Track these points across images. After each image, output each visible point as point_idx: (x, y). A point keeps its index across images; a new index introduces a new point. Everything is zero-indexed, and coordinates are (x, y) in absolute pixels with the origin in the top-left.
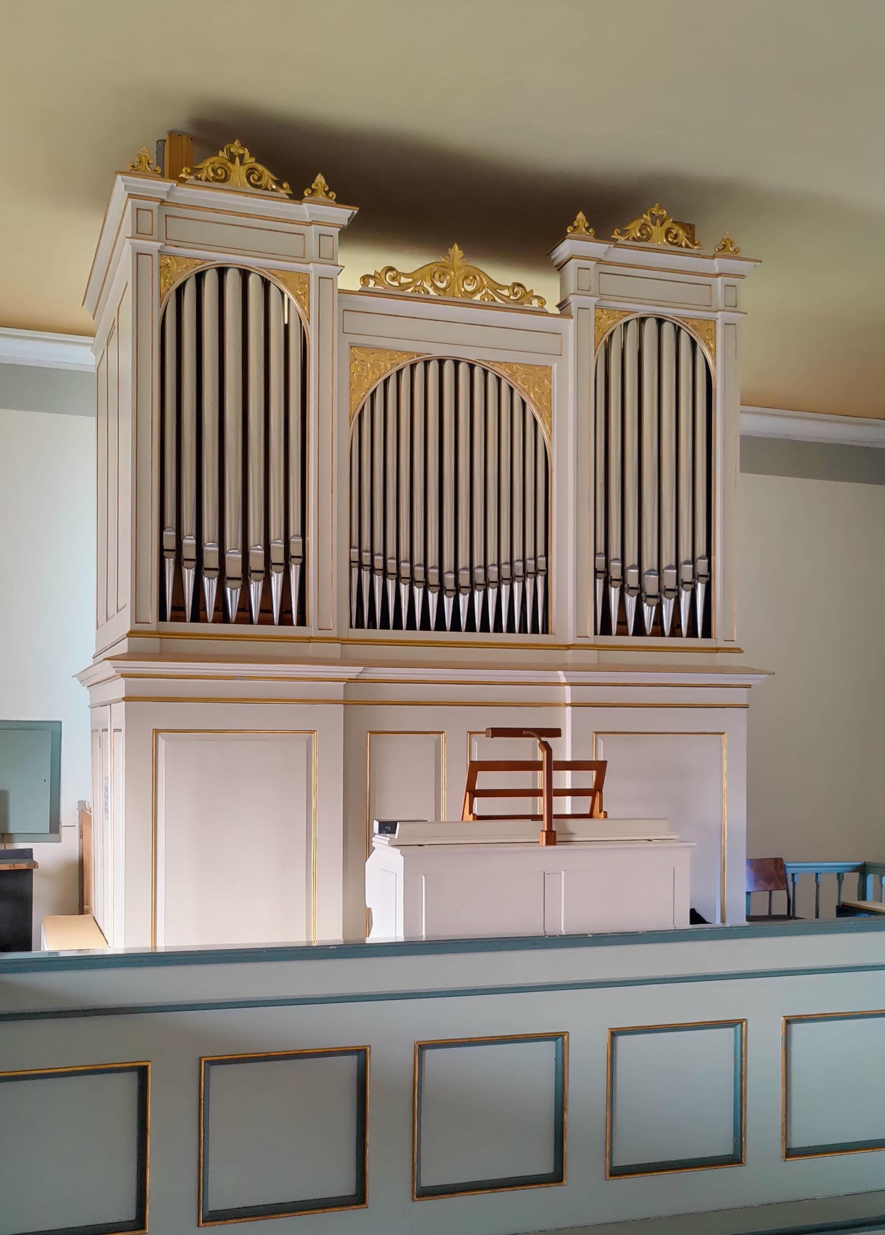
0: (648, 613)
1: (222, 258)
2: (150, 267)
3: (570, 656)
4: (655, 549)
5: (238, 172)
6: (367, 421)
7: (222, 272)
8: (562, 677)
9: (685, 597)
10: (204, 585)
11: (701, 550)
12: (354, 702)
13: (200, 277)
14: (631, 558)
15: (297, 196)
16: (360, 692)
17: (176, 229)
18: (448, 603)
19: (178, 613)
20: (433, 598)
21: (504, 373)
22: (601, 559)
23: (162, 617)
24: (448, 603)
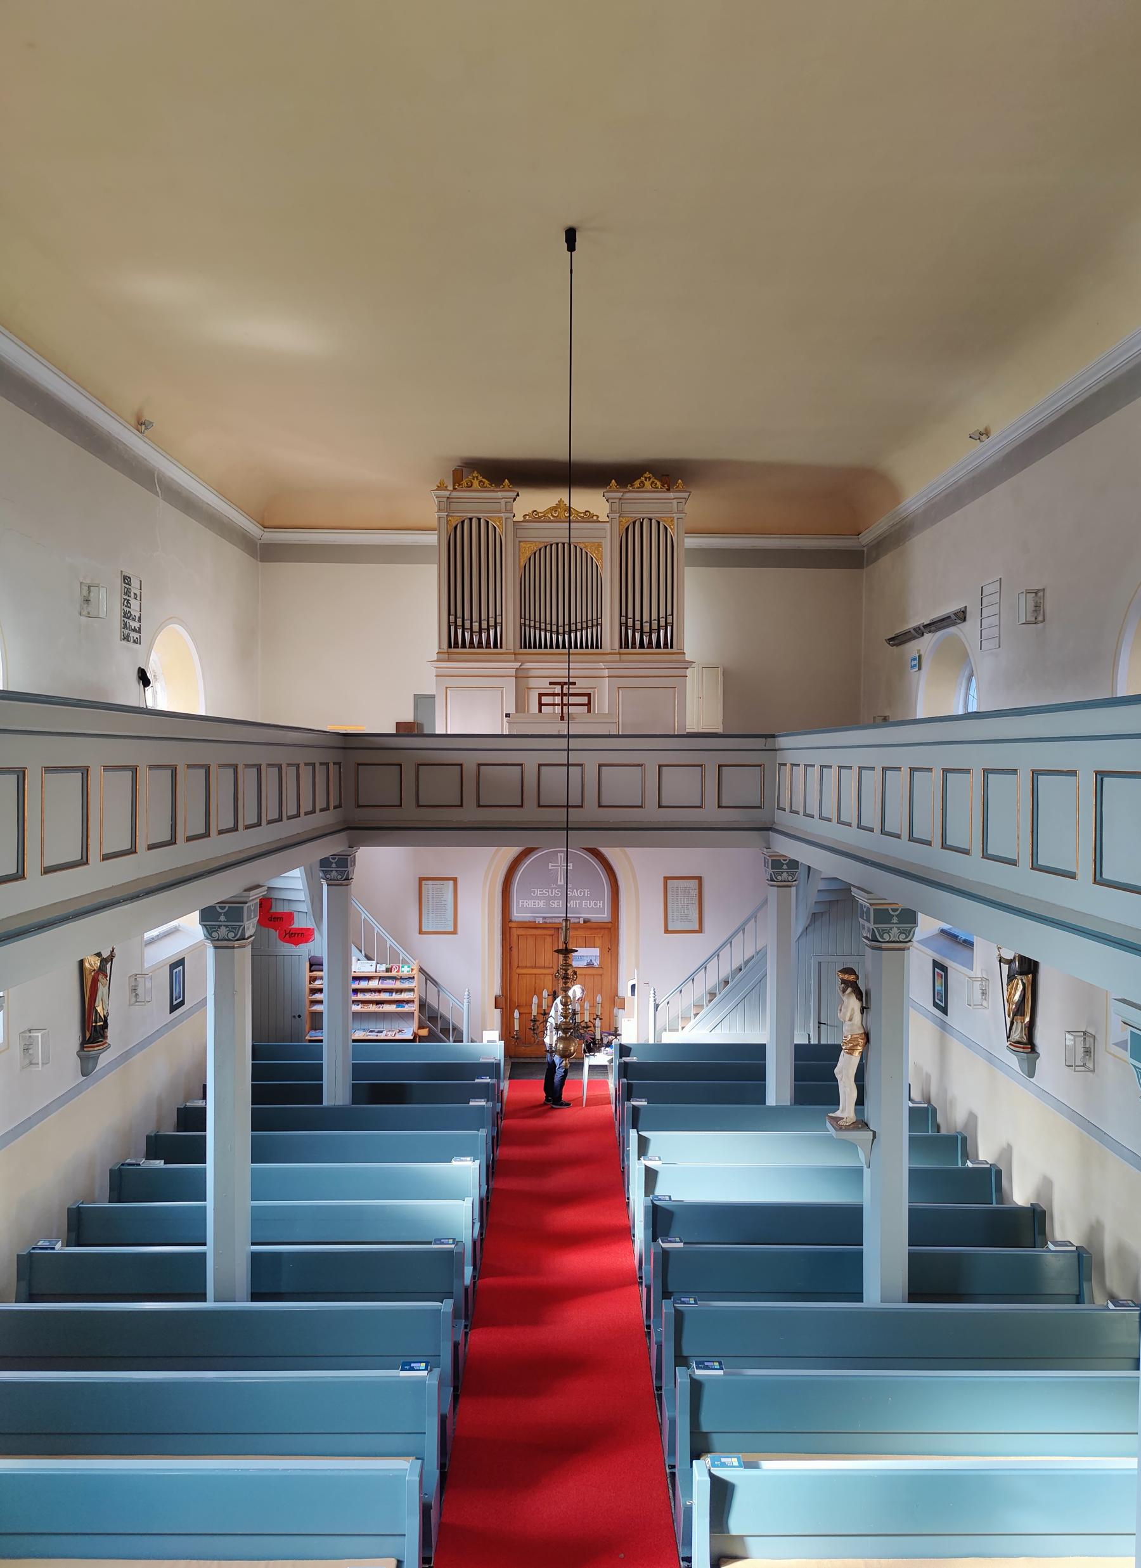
1: (470, 515)
2: (444, 522)
3: (608, 658)
4: (649, 613)
5: (476, 483)
6: (528, 569)
7: (471, 519)
8: (602, 665)
9: (662, 633)
10: (465, 634)
11: (669, 612)
12: (520, 676)
13: (463, 522)
14: (638, 617)
15: (498, 485)
16: (521, 673)
17: (454, 506)
18: (560, 638)
19: (456, 646)
20: (554, 636)
21: (582, 546)
22: (623, 619)
23: (450, 646)
24: (560, 638)
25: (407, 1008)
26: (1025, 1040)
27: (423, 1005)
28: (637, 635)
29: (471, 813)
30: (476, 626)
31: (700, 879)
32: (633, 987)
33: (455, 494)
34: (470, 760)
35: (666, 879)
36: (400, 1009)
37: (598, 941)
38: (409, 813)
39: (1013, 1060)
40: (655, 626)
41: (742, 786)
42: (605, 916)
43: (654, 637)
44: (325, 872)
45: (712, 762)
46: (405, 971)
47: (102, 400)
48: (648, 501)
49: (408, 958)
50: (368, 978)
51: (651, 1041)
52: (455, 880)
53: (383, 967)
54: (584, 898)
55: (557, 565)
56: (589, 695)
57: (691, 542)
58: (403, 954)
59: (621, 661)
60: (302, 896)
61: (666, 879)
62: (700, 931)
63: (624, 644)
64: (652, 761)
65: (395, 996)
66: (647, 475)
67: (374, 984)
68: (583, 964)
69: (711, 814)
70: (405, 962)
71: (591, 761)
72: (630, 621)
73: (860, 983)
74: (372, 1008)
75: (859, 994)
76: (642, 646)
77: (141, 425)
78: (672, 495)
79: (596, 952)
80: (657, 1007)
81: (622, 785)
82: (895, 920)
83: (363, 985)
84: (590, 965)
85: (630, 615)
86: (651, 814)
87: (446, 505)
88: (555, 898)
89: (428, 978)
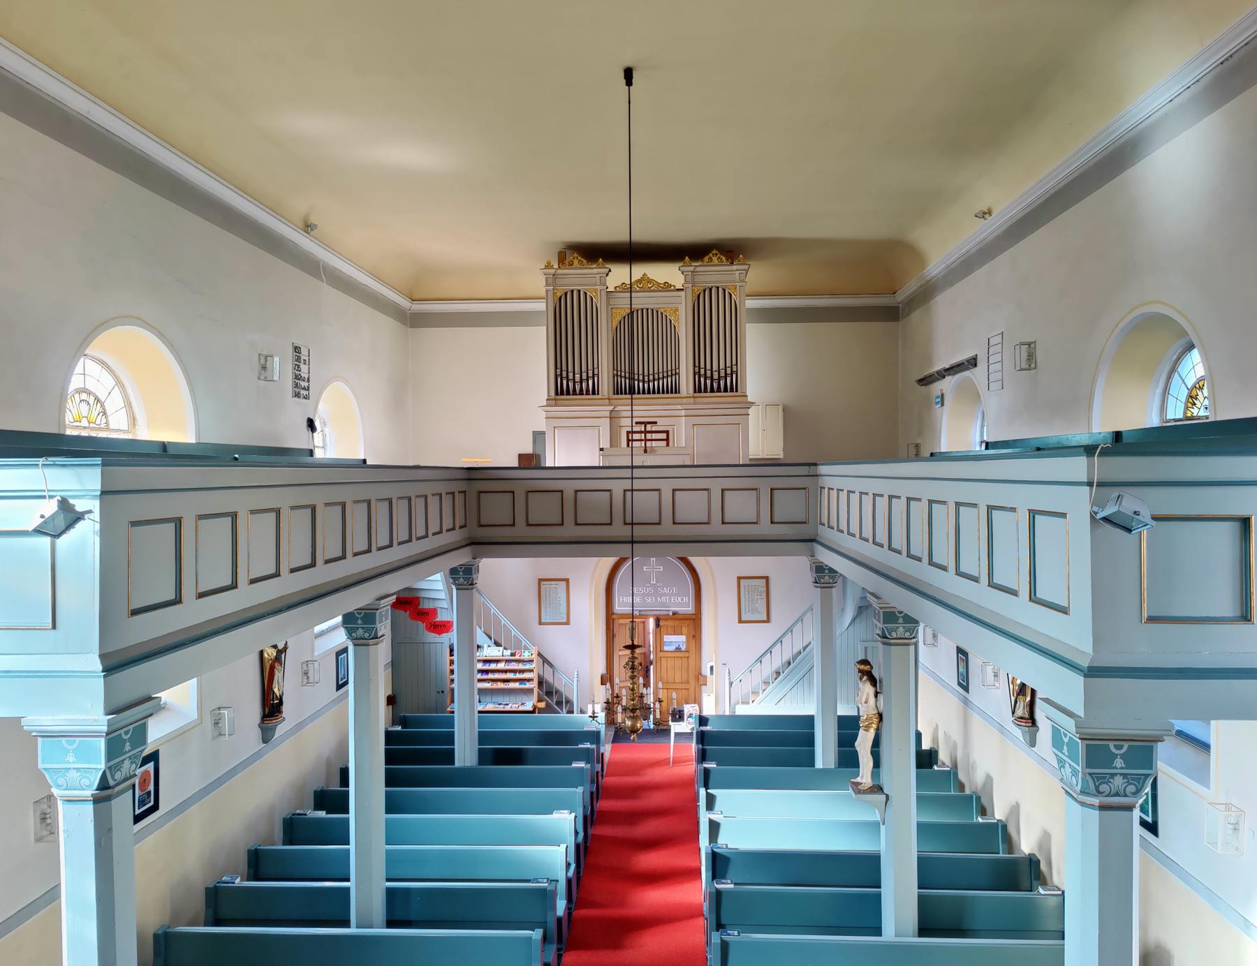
0: (715, 385)
2: (550, 294)
4: (718, 363)
5: (576, 262)
9: (729, 379)
10: (568, 385)
12: (613, 417)
14: (708, 367)
16: (614, 414)
25: (528, 685)
26: (1027, 716)
27: (541, 683)
28: (709, 382)
29: (570, 531)
30: (578, 377)
31: (767, 578)
32: (712, 668)
33: (560, 271)
34: (569, 487)
35: (739, 578)
36: (522, 686)
37: (685, 630)
38: (521, 531)
39: (1017, 732)
40: (722, 374)
41: (790, 505)
42: (689, 609)
43: (722, 383)
44: (454, 579)
45: (765, 486)
46: (526, 655)
47: (275, 211)
48: (713, 272)
49: (529, 645)
50: (497, 661)
51: (727, 713)
52: (567, 580)
53: (508, 653)
54: (673, 594)
55: (633, 327)
56: (667, 432)
57: (751, 303)
58: (525, 642)
59: (695, 403)
60: (442, 595)
61: (739, 578)
62: (768, 621)
63: (698, 389)
64: (716, 486)
65: (518, 676)
66: (715, 252)
67: (501, 666)
68: (673, 648)
69: (765, 528)
70: (526, 648)
71: (666, 487)
72: (702, 371)
73: (875, 673)
74: (501, 685)
75: (873, 681)
76: (712, 390)
77: (308, 227)
78: (734, 267)
79: (682, 638)
80: (731, 684)
81: (692, 506)
82: (901, 621)
83: (493, 666)
84: (678, 649)
85: (702, 365)
86: (716, 529)
87: (552, 280)
88: (649, 595)
89: (545, 661)
